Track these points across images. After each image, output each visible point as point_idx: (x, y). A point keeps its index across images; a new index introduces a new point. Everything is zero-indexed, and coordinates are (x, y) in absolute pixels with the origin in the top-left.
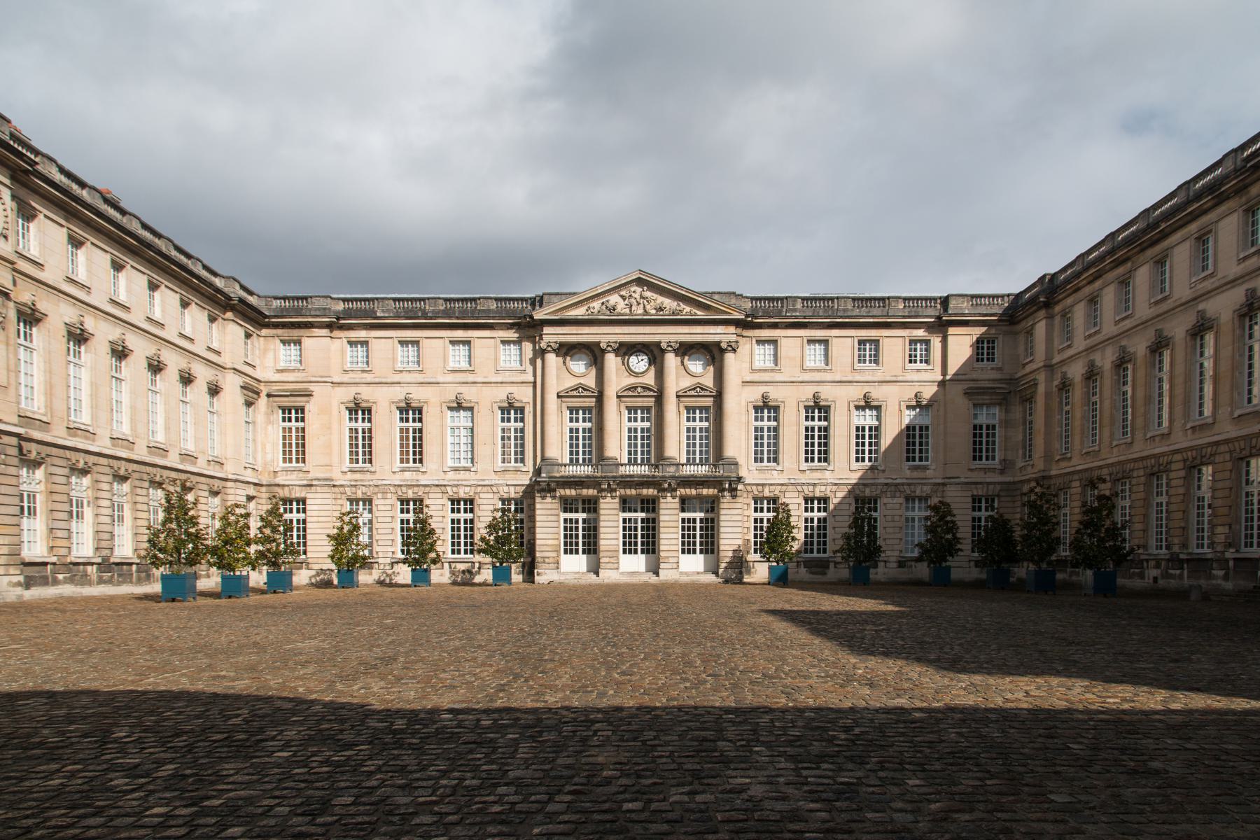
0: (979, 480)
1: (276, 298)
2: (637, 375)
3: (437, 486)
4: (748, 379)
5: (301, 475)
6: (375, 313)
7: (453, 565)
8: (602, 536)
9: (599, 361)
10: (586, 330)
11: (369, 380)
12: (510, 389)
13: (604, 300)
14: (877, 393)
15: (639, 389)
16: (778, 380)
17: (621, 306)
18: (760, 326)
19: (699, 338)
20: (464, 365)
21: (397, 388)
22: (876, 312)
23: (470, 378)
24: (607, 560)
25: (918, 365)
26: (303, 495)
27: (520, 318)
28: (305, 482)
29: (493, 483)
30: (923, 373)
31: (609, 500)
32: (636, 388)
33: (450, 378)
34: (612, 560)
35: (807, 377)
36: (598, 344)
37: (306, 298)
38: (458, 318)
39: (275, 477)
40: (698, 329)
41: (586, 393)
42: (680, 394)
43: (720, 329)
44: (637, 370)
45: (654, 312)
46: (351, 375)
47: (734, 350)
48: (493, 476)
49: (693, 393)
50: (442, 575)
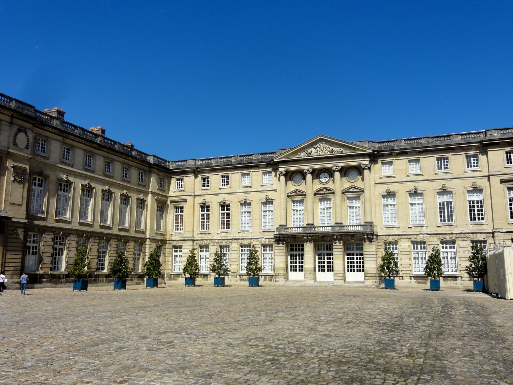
1: (175, 162)
2: (323, 183)
3: (235, 239)
5: (181, 235)
6: (212, 164)
7: (241, 277)
8: (305, 262)
11: (209, 193)
14: (449, 184)
15: (324, 190)
16: (394, 181)
18: (382, 156)
20: (248, 184)
21: (220, 196)
22: (445, 143)
23: (249, 189)
24: (308, 275)
25: (473, 168)
27: (270, 161)
28: (182, 239)
29: (258, 237)
30: (475, 172)
31: (308, 244)
32: (322, 190)
34: (310, 275)
35: (409, 179)
36: (303, 170)
37: (186, 161)
38: (244, 164)
39: (172, 237)
42: (344, 191)
45: (329, 153)
46: (202, 191)
47: (369, 169)
49: (350, 190)
50: (236, 281)
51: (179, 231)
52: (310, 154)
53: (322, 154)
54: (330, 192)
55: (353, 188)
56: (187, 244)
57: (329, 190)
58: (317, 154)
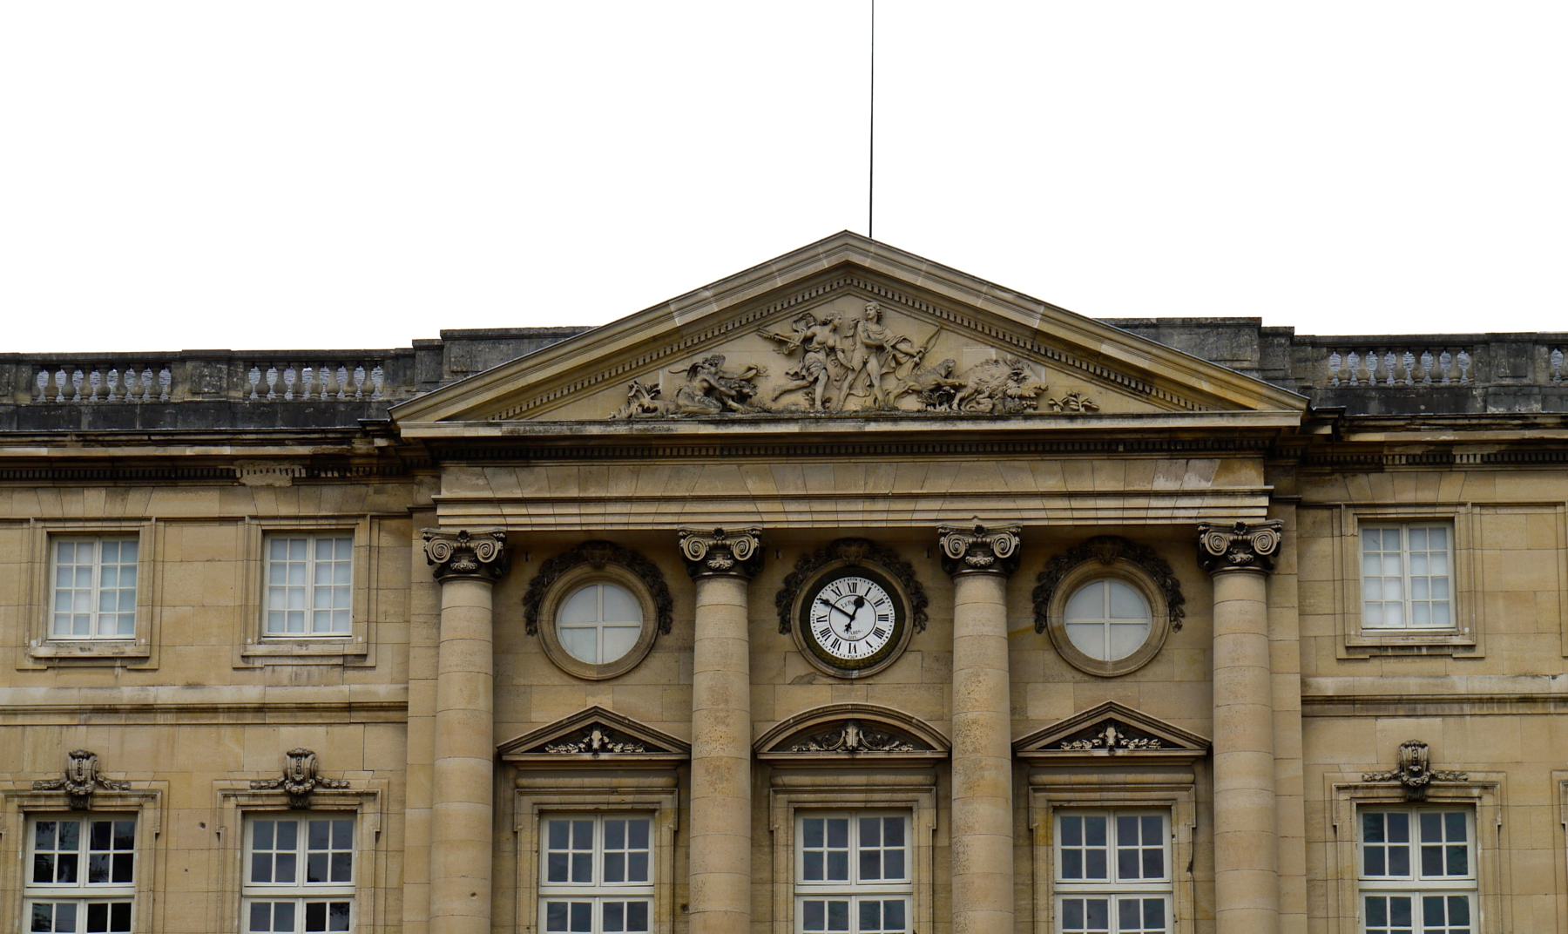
2: (844, 670)
4: (1329, 685)
9: (678, 614)
12: (294, 736)
13: (698, 359)
15: (851, 736)
17: (776, 371)
18: (1373, 461)
19: (1107, 513)
20: (108, 633)
23: (129, 690)
27: (346, 438)
33: (39, 690)
38: (85, 440)
40: (1105, 475)
41: (617, 752)
42: (1032, 752)
43: (1196, 475)
44: (843, 652)
45: (911, 404)
47: (1265, 566)
52: (742, 398)
53: (853, 405)
54: (907, 752)
55: (1111, 733)
57: (906, 738)
58: (800, 400)
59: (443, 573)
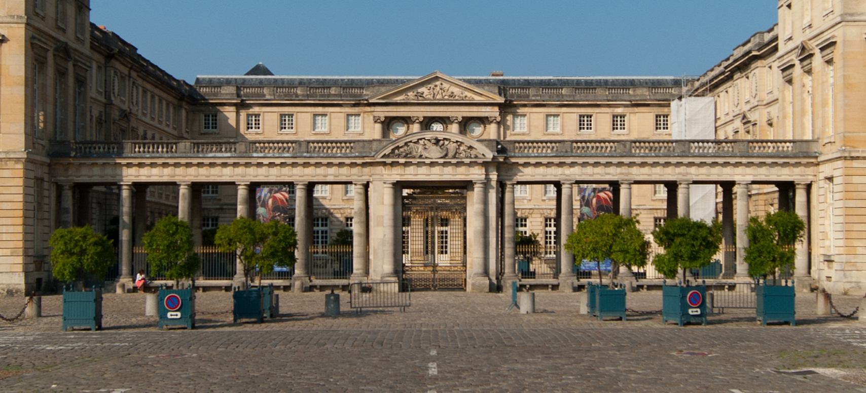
0: (659, 207)
10: (402, 109)
18: (515, 106)
26: (217, 215)
28: (218, 207)
29: (341, 207)
40: (475, 109)
43: (488, 109)
48: (341, 203)
51: (210, 194)
53: (438, 97)
56: (227, 215)
59: (375, 122)
